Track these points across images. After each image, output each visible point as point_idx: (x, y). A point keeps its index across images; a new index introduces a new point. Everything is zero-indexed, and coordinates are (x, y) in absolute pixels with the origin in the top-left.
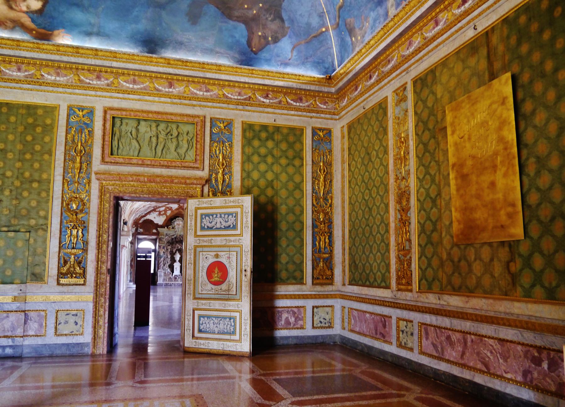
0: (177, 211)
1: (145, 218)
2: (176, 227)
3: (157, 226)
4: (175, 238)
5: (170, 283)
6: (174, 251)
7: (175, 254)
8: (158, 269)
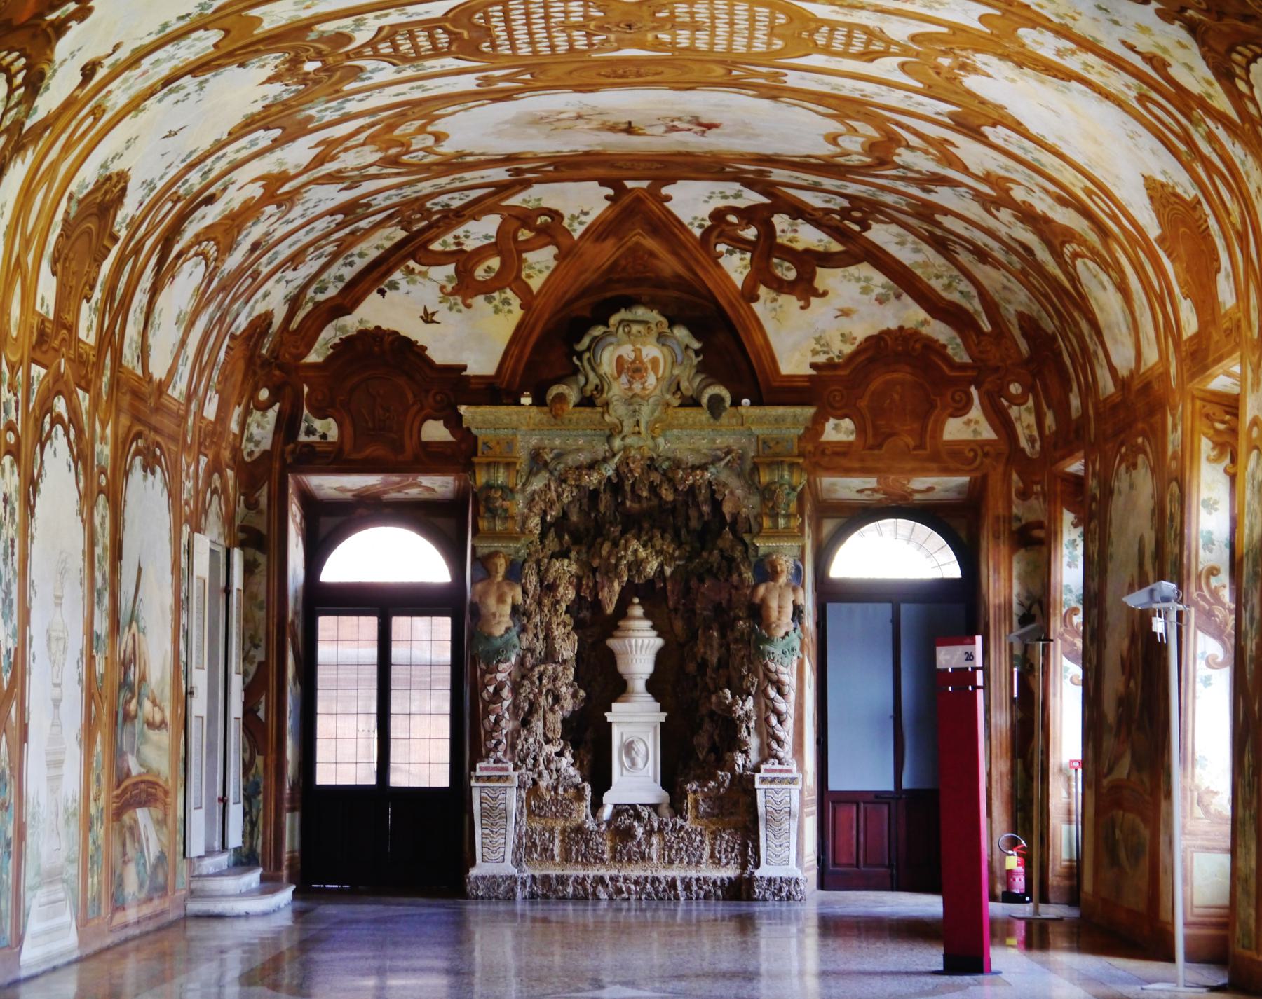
0: (608, 251)
1: (351, 323)
2: (617, 390)
3: (453, 387)
4: (615, 486)
6: (610, 596)
7: (613, 623)
8: (478, 756)
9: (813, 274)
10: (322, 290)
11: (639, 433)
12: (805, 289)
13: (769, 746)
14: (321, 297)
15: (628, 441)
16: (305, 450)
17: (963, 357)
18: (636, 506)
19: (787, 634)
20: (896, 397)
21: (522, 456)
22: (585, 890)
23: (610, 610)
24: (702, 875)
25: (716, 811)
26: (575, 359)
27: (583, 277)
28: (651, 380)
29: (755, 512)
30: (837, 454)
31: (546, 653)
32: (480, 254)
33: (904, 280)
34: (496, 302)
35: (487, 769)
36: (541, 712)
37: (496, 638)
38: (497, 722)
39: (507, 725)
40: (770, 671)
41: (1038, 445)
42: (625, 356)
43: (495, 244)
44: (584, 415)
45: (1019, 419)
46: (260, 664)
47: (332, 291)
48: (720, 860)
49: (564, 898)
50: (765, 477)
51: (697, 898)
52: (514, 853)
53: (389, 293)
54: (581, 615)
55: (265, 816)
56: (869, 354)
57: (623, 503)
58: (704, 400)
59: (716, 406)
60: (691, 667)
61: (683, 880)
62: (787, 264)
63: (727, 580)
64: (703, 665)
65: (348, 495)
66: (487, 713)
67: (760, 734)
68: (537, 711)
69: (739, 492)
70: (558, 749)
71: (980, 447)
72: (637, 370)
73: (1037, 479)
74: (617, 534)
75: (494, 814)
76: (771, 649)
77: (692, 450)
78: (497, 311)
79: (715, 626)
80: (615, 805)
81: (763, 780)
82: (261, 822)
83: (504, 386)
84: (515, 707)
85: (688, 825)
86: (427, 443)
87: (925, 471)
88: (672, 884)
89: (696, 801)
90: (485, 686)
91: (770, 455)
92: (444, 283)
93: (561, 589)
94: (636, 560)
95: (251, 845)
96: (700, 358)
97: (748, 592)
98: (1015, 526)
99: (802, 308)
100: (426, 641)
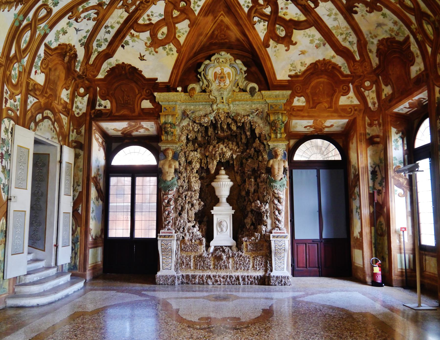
1: (113, 61)
2: (214, 86)
3: (153, 85)
4: (214, 125)
5: (199, 273)
6: (213, 167)
7: (214, 177)
8: (163, 228)
9: (292, 33)
10: (99, 45)
11: (223, 102)
12: (287, 41)
13: (275, 223)
14: (100, 49)
15: (218, 106)
16: (98, 112)
17: (347, 71)
18: (222, 134)
19: (281, 179)
20: (321, 88)
21: (179, 113)
22: (203, 281)
23: (213, 172)
24: (249, 274)
25: (255, 249)
26: (198, 75)
27: (201, 38)
28: (228, 82)
29: (268, 132)
30: (298, 110)
31: (188, 188)
32: (159, 24)
33: (328, 36)
34: (167, 50)
35: (164, 233)
36: (186, 210)
37: (168, 181)
38: (168, 214)
39: (173, 215)
40: (275, 193)
41: (377, 105)
42: (218, 72)
43: (164, 19)
44: (202, 96)
45: (368, 96)
46: (80, 192)
47: (104, 47)
48: (256, 268)
49: (195, 284)
50: (272, 118)
51: (248, 284)
52: (175, 266)
53: (126, 47)
54: (202, 175)
55: (80, 250)
56: (311, 71)
57: (218, 133)
58: (248, 89)
59: (252, 91)
60: (243, 193)
61: (242, 277)
62: (282, 28)
63: (257, 159)
64: (248, 192)
65: (119, 133)
66: (165, 211)
68: (184, 210)
69: (261, 125)
70: (193, 225)
71: (353, 107)
72: (222, 77)
73: (375, 119)
74: (215, 143)
76: (276, 185)
77: (244, 110)
78: (168, 54)
79: (253, 177)
80: (215, 246)
82: (78, 253)
83: (172, 86)
84: (176, 208)
85: (243, 255)
86: (143, 109)
87: (332, 117)
88: (238, 278)
89: (247, 245)
90: (164, 200)
91: (273, 109)
93: (194, 163)
94: (222, 152)
95: (75, 262)
96: (246, 75)
97: (266, 163)
98: (368, 137)
99: (286, 50)
100: (148, 185)
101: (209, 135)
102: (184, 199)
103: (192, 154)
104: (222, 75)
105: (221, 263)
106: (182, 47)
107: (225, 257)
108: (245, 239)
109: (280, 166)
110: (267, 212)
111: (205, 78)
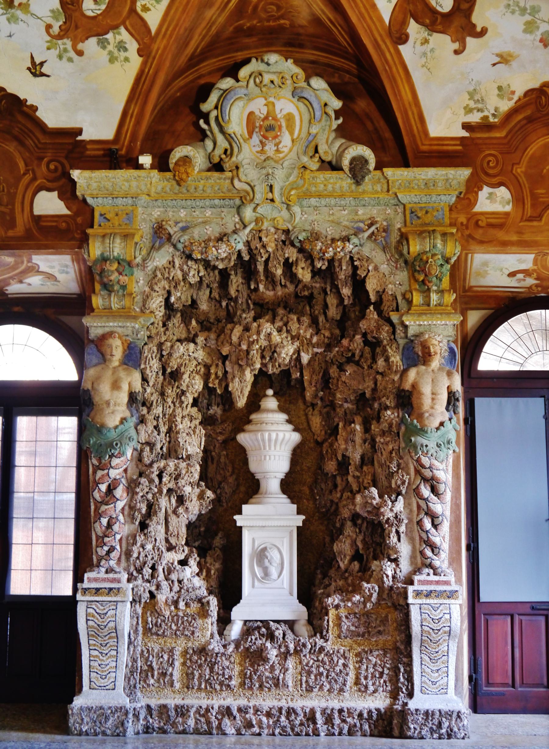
2: (247, 154)
3: (69, 150)
4: (247, 267)
5: (196, 700)
6: (241, 389)
7: (243, 419)
11: (272, 200)
13: (422, 553)
15: (259, 209)
18: (270, 293)
19: (442, 424)
22: (209, 723)
23: (241, 402)
24: (345, 705)
25: (362, 630)
26: (201, 122)
27: (210, 13)
28: (286, 140)
29: (403, 289)
31: (169, 449)
34: (110, 47)
35: (96, 580)
36: (161, 515)
37: (109, 430)
38: (109, 526)
40: (423, 467)
42: (257, 113)
44: (211, 181)
48: (366, 687)
49: (184, 732)
50: (415, 247)
51: (340, 734)
52: (128, 679)
54: (211, 412)
56: (528, 112)
57: (256, 289)
58: (346, 163)
59: (358, 170)
60: (331, 466)
61: (323, 712)
63: (370, 367)
64: (344, 464)
66: (99, 516)
67: (411, 540)
68: (156, 513)
70: (182, 557)
72: (270, 128)
74: (249, 320)
75: (107, 634)
76: (425, 442)
77: (333, 222)
78: (112, 59)
79: (358, 419)
80: (246, 622)
81: (418, 594)
83: (123, 152)
85: (329, 646)
86: (40, 217)
88: (311, 717)
89: (339, 618)
90: (97, 484)
91: (418, 222)
92: (50, 21)
93: (186, 376)
94: (270, 346)
96: (340, 121)
97: (396, 378)
99: (456, 52)
101: (231, 293)
102: (157, 480)
103: (181, 349)
104: (270, 121)
105: (264, 670)
106: (153, 39)
107: (275, 652)
108: (334, 600)
109: (437, 385)
110: (400, 521)
111: (222, 130)
